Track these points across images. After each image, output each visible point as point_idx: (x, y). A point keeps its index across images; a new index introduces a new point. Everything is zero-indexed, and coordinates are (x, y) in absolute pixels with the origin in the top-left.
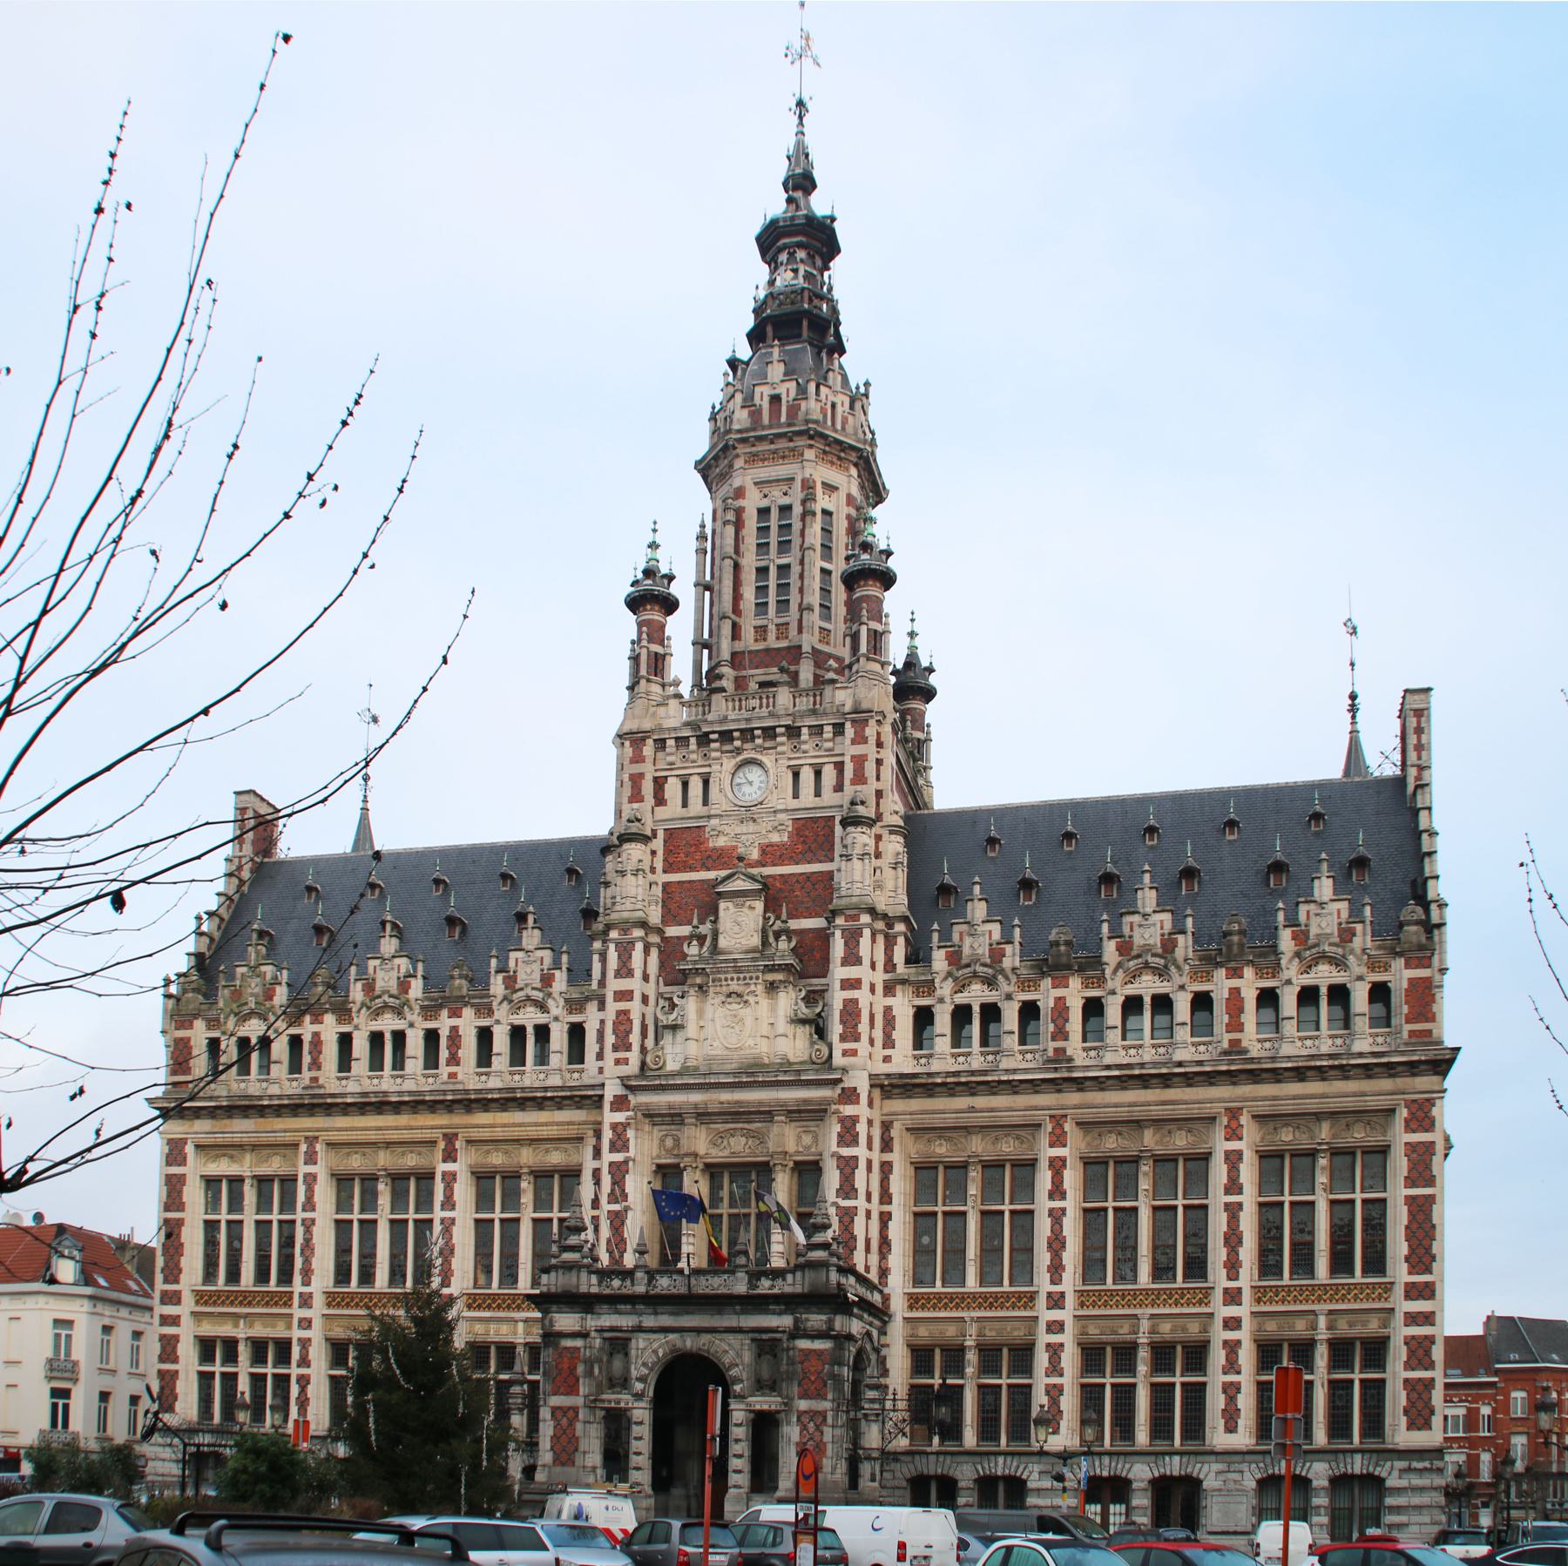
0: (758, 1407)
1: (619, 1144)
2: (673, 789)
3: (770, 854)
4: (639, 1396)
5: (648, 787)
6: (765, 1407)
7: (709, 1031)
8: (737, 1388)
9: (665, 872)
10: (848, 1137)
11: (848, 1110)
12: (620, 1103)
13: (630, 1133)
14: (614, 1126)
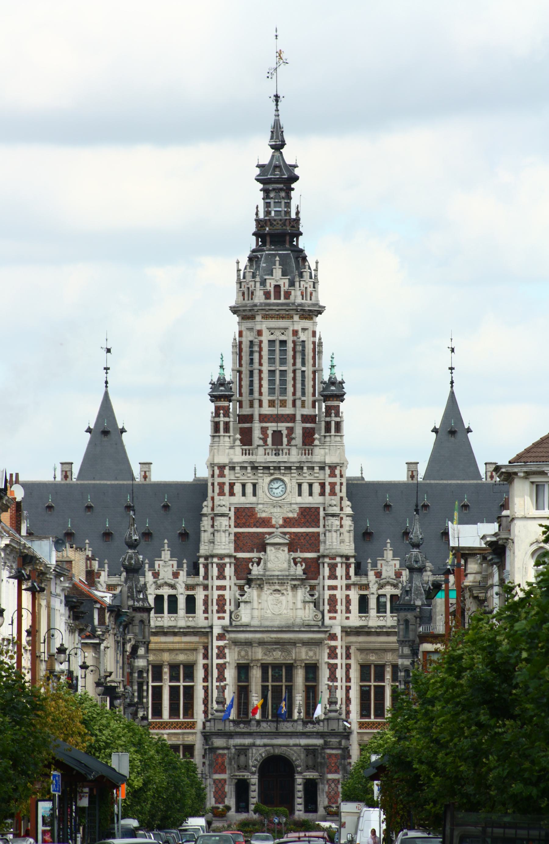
0: (308, 777)
1: (221, 655)
2: (238, 488)
3: (288, 522)
4: (253, 773)
5: (227, 489)
6: (311, 777)
7: (264, 605)
8: (299, 769)
9: (235, 527)
10: (333, 655)
11: (333, 643)
12: (221, 637)
13: (227, 651)
14: (218, 647)
